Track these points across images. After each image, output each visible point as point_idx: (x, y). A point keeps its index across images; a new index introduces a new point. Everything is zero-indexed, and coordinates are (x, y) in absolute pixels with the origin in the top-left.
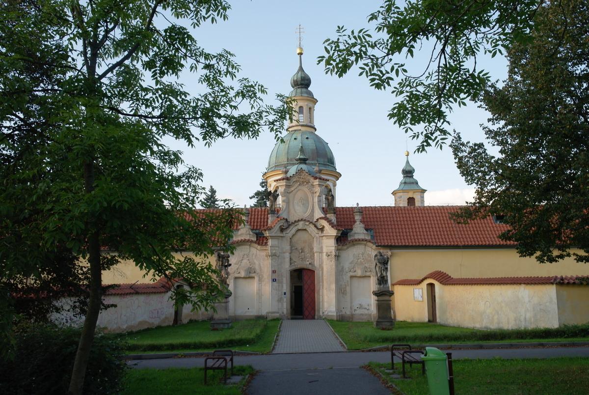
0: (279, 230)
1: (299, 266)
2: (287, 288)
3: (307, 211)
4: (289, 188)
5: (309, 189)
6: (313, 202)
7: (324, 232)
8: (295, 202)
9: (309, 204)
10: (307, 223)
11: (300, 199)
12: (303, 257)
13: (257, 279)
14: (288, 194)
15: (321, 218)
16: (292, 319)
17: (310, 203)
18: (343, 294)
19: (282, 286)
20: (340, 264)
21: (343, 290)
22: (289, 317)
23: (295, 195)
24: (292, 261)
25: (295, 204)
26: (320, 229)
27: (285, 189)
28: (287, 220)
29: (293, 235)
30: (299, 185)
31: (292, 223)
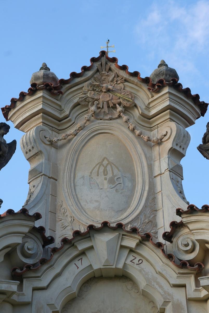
3: (128, 204)
4: (59, 131)
5: (133, 131)
6: (152, 177)
8: (79, 174)
9: (133, 180)
10: (131, 243)
11: (101, 164)
14: (53, 150)
17: (139, 180)
23: (78, 152)
25: (79, 181)
26: (191, 263)
27: (39, 131)
30: (96, 115)
31: (65, 241)
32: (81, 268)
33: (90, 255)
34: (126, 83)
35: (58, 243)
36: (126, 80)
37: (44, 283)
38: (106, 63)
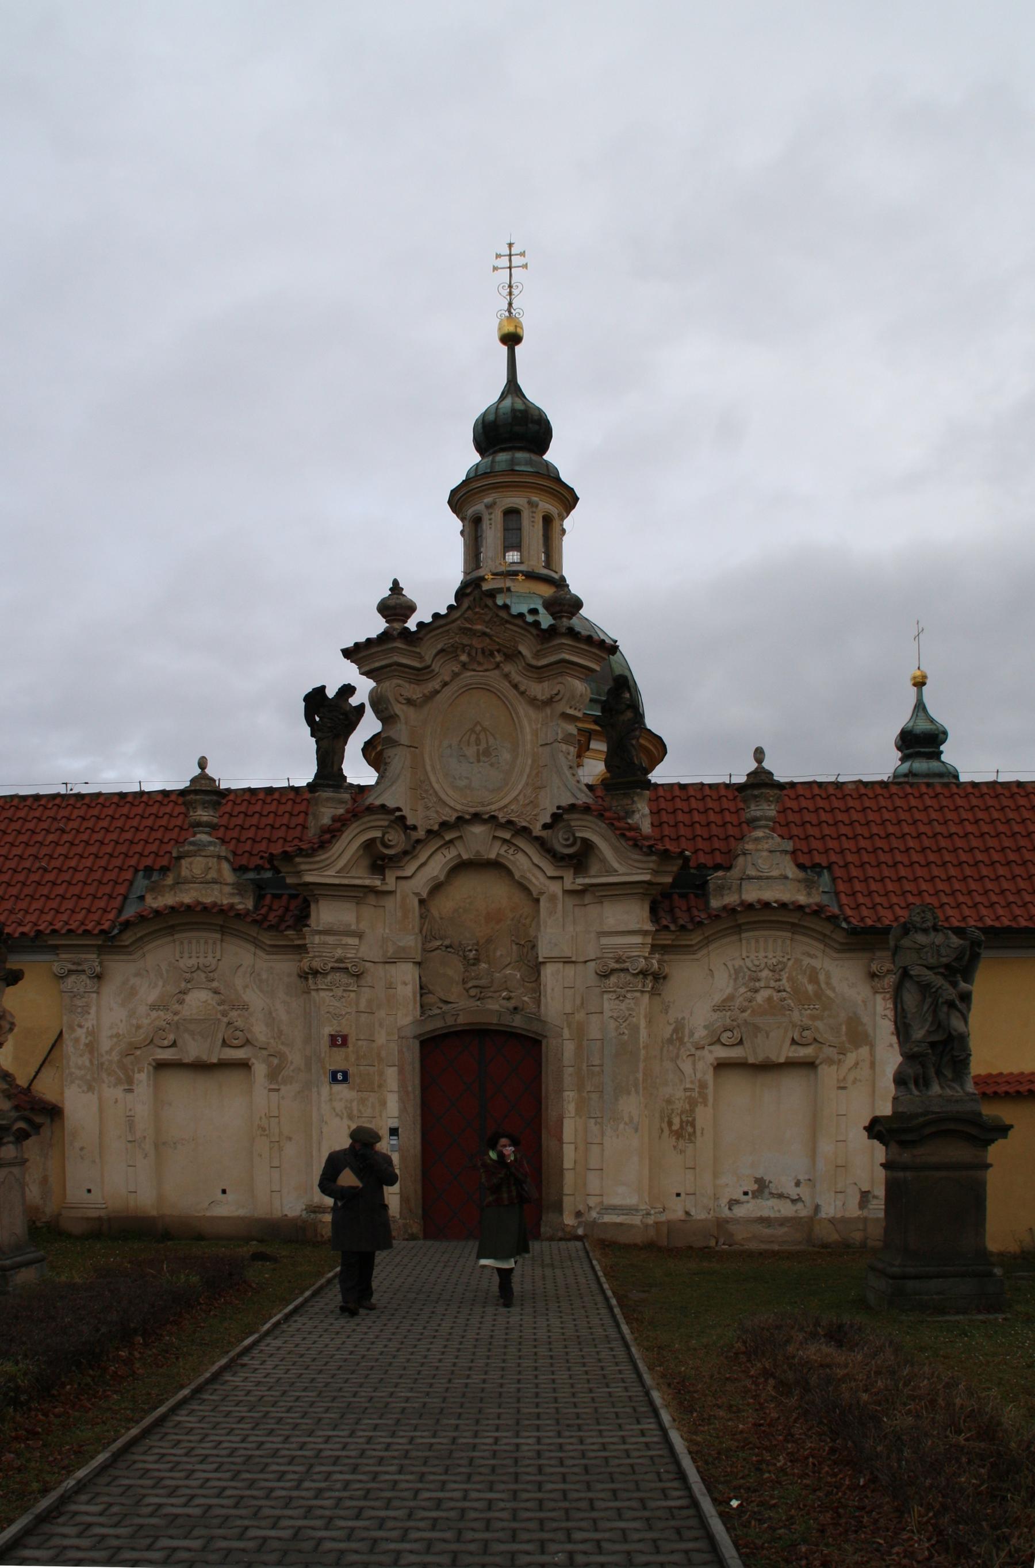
0: (365, 862)
1: (461, 1020)
2: (403, 1110)
7: (594, 869)
12: (482, 982)
13: (260, 1069)
15: (573, 808)
16: (426, 1237)
18: (678, 1135)
19: (383, 1103)
20: (666, 1010)
21: (676, 1121)
22: (416, 1229)
24: (430, 999)
28: (403, 818)
29: (437, 888)
31: (429, 832)
32: (449, 857)
33: (457, 843)
34: (508, 626)
35: (421, 834)
36: (507, 622)
37: (408, 872)
38: (481, 599)
